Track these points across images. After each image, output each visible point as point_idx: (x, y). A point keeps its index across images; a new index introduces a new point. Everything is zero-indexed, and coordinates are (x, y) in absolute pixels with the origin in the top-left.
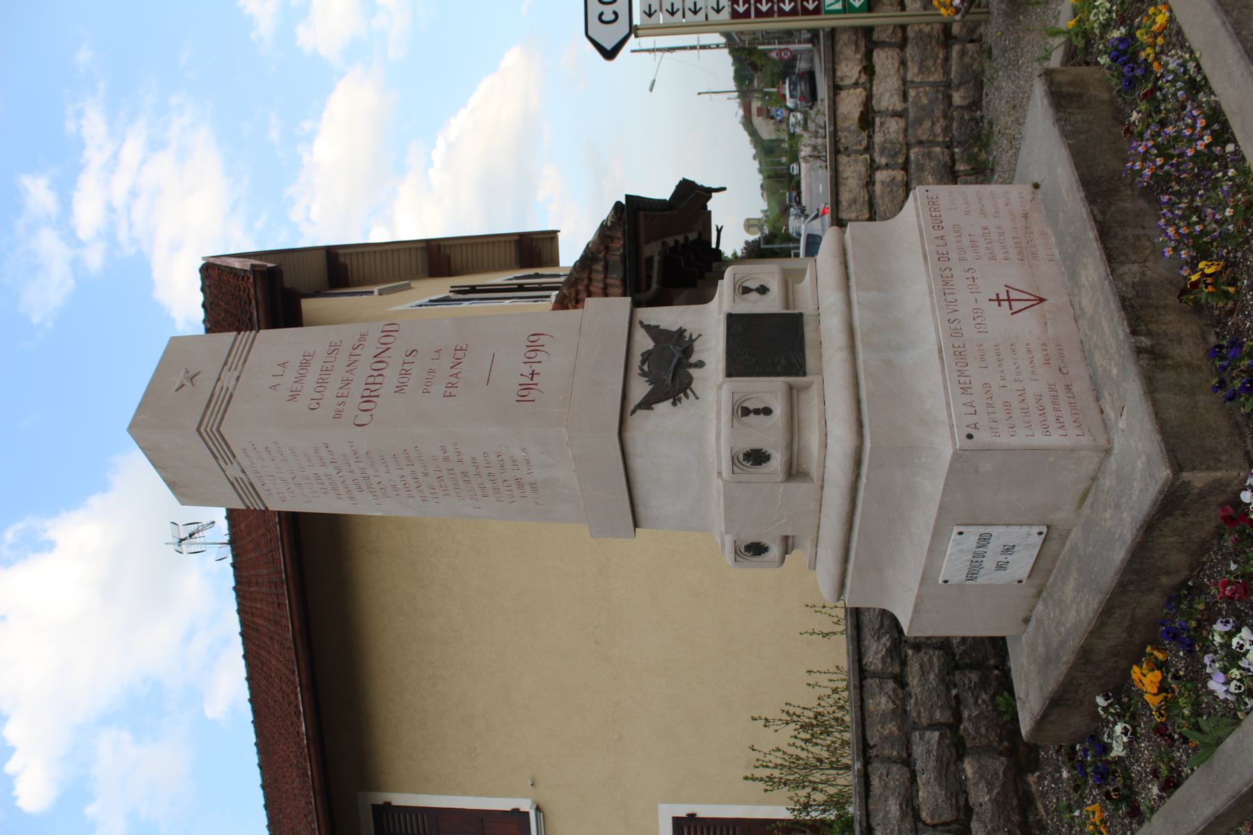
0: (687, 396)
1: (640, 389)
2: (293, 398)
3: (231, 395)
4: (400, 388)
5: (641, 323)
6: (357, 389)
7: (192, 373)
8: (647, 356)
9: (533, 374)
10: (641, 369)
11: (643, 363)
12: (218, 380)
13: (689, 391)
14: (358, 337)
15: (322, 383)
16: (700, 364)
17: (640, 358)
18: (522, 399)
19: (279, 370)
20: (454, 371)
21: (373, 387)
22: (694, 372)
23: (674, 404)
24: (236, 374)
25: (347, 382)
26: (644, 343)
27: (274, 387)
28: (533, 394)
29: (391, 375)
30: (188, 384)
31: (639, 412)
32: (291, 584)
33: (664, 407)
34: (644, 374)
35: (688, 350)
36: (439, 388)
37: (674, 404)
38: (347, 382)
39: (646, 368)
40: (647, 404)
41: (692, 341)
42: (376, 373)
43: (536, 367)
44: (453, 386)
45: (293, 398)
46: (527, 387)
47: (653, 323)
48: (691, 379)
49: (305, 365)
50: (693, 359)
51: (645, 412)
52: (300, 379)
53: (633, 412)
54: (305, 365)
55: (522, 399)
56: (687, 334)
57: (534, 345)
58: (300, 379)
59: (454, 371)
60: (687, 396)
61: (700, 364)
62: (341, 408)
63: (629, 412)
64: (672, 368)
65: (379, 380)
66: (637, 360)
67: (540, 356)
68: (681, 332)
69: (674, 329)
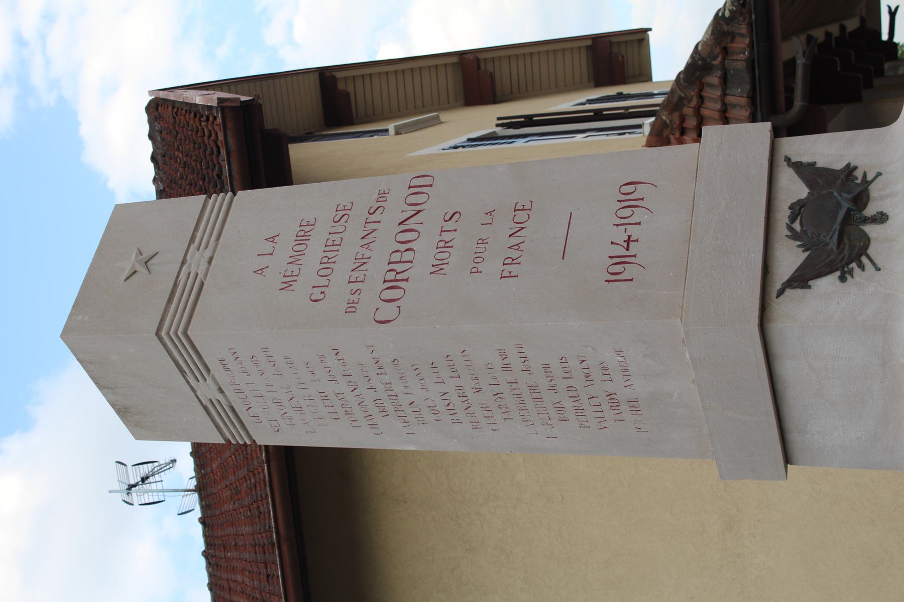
0: (862, 267)
1: (790, 258)
2: (287, 285)
3: (202, 284)
4: (438, 268)
5: (788, 159)
6: (377, 270)
7: (147, 254)
8: (797, 209)
9: (628, 241)
10: (790, 228)
11: (793, 219)
12: (183, 263)
13: (864, 259)
14: (375, 196)
15: (327, 263)
16: (881, 218)
17: (789, 212)
18: (614, 278)
19: (268, 247)
21: (399, 267)
22: (870, 230)
23: (842, 279)
24: (208, 254)
25: (362, 262)
26: (793, 189)
27: (260, 271)
28: (630, 271)
29: (425, 249)
30: (141, 269)
31: (789, 292)
32: (284, 547)
33: (827, 284)
34: (794, 236)
35: (861, 198)
36: (493, 266)
37: (842, 279)
38: (362, 262)
39: (797, 226)
40: (801, 279)
41: (866, 183)
42: (403, 247)
43: (633, 231)
44: (514, 262)
45: (287, 285)
46: (621, 261)
47: (806, 159)
48: (867, 240)
49: (302, 238)
50: (870, 210)
51: (799, 292)
52: (295, 259)
53: (781, 293)
54: (302, 238)
55: (614, 278)
56: (859, 174)
57: (630, 198)
58: (295, 259)
59: (514, 241)
60: (862, 267)
61: (881, 218)
62: (355, 297)
63: (774, 294)
64: (837, 226)
65: (408, 256)
67: (639, 215)
68: (850, 170)
69: (839, 166)
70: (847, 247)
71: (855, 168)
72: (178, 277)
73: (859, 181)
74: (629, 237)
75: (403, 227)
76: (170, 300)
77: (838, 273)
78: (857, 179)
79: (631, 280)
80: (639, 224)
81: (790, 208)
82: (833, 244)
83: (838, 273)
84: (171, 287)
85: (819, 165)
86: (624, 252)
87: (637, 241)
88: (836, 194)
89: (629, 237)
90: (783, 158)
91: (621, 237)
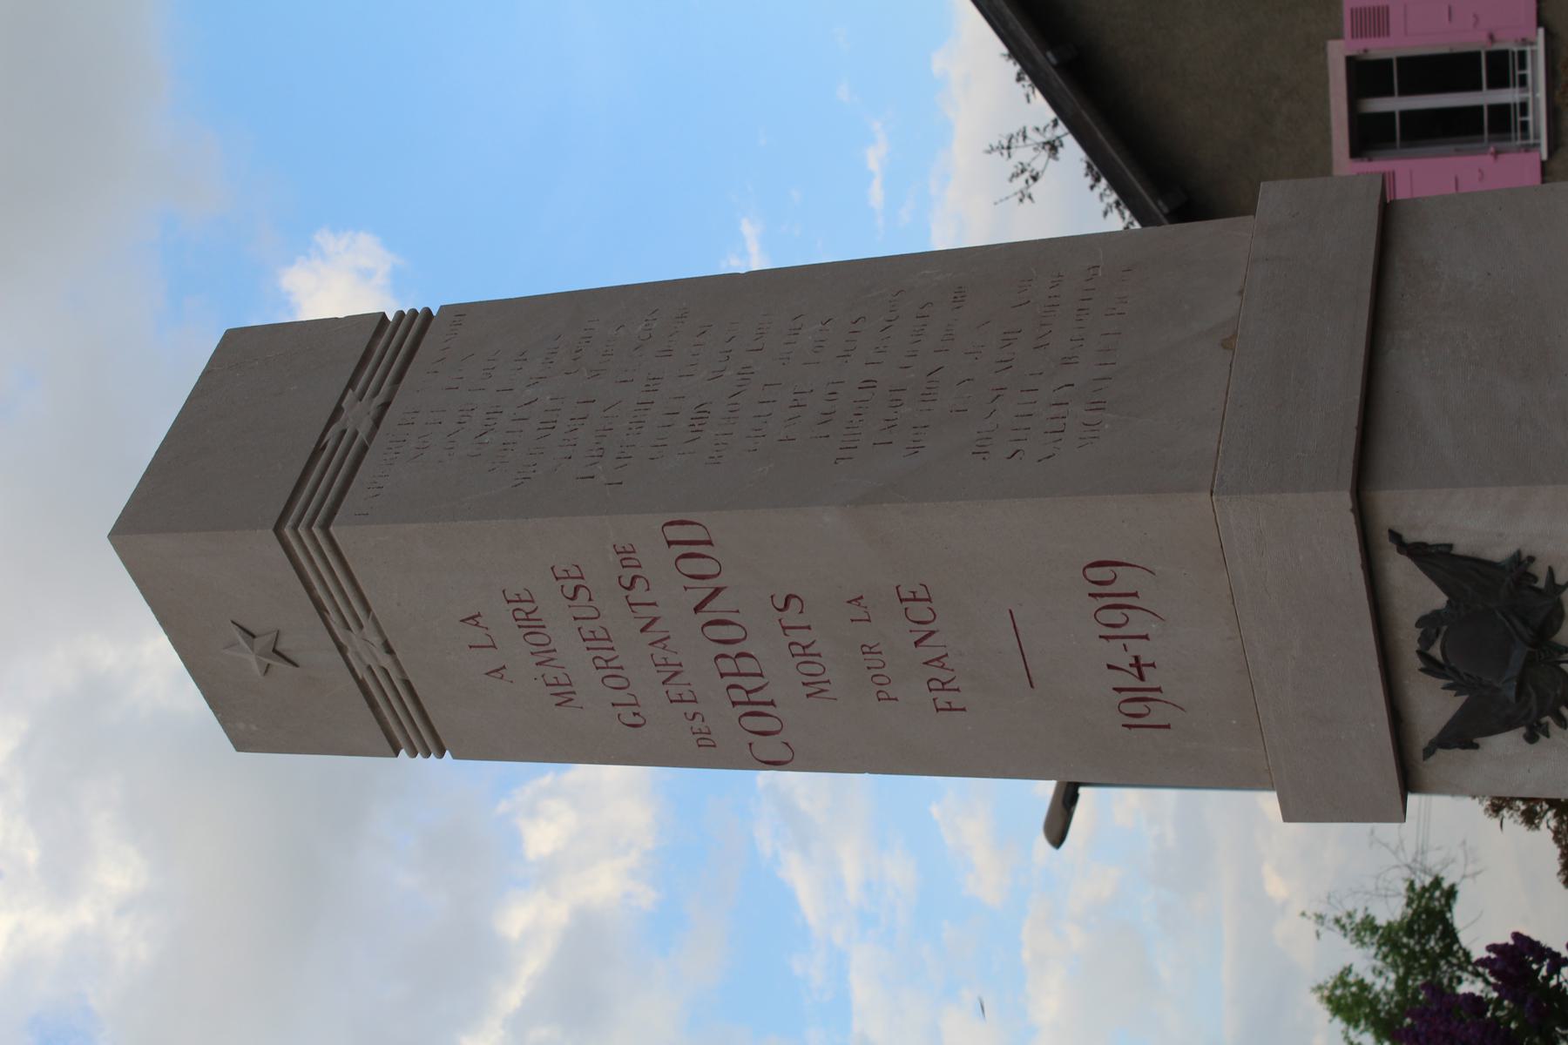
2: (565, 696)
3: (407, 684)
4: (816, 688)
5: (1395, 537)
8: (1430, 624)
10: (1422, 654)
11: (1426, 641)
12: (341, 649)
14: (613, 558)
17: (1417, 632)
18: (1134, 723)
20: (926, 653)
24: (376, 640)
28: (1158, 714)
31: (1441, 753)
34: (1432, 667)
43: (1146, 652)
45: (565, 696)
47: (1431, 536)
49: (530, 624)
51: (1458, 753)
52: (545, 656)
53: (1429, 752)
55: (1134, 723)
57: (1109, 587)
58: (545, 656)
59: (926, 653)
63: (1419, 754)
66: (1408, 638)
70: (1534, 696)
71: (1531, 559)
72: (352, 670)
73: (1541, 584)
74: (1137, 658)
75: (705, 617)
76: (373, 705)
77: (1523, 730)
78: (1536, 579)
79: (1168, 727)
80: (1146, 637)
81: (1418, 625)
82: (1512, 694)
83: (1523, 730)
84: (358, 690)
85: (1461, 549)
86: (1134, 682)
87: (1153, 665)
88: (1499, 616)
89: (1137, 658)
90: (1386, 533)
91: (1125, 660)
